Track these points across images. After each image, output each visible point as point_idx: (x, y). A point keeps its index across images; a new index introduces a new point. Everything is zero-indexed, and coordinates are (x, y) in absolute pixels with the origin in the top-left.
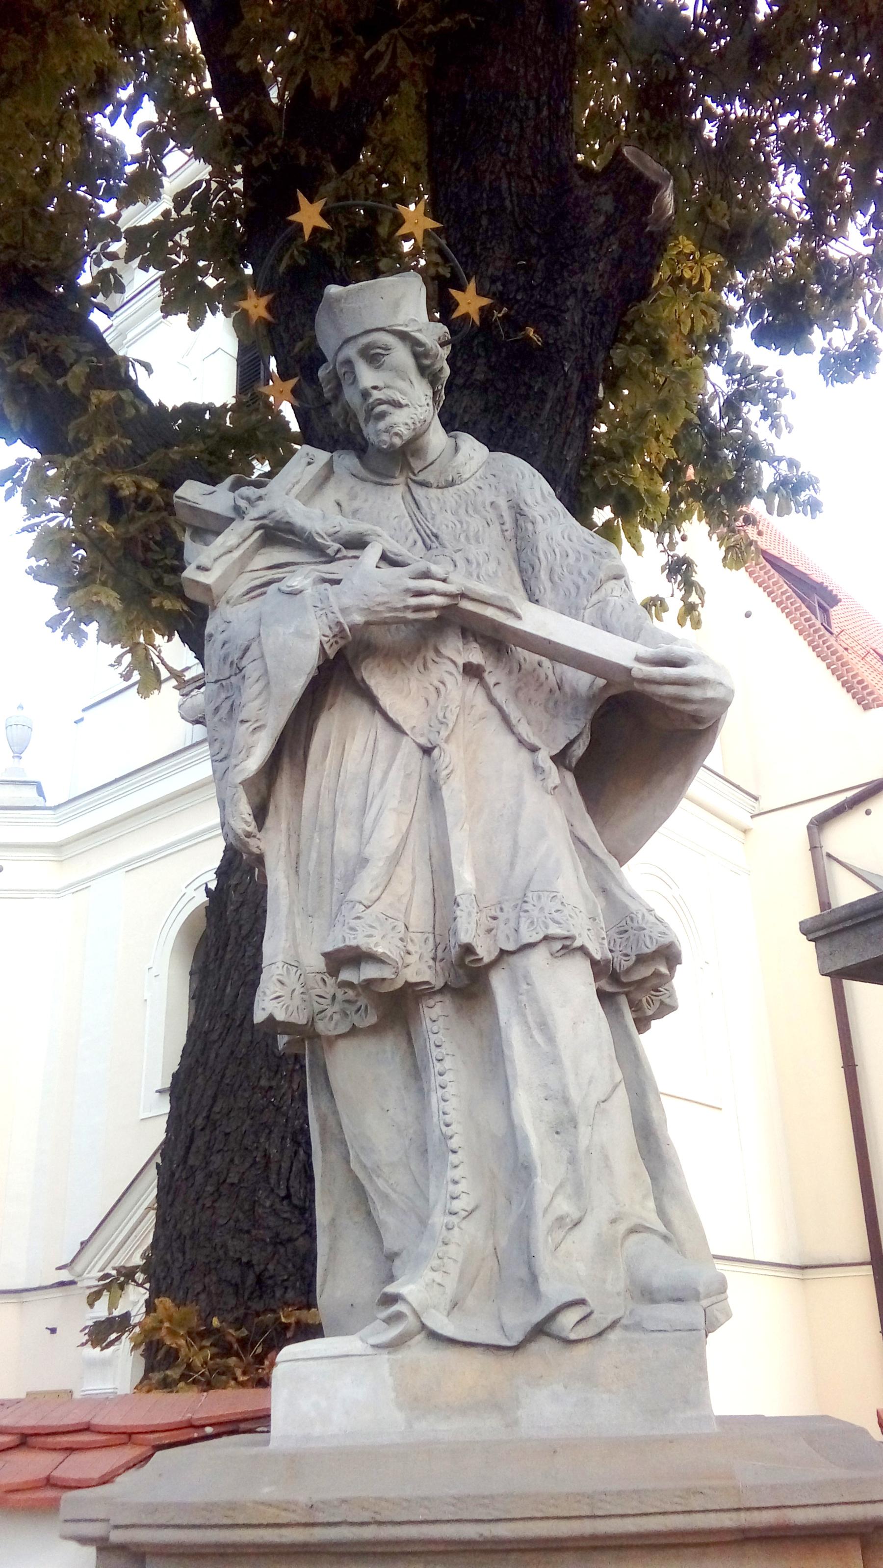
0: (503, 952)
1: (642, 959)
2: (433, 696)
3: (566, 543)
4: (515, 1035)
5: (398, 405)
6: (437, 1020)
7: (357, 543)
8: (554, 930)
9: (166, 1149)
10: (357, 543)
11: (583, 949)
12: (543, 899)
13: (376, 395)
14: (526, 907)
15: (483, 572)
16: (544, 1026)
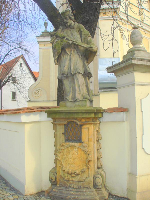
0: (74, 74)
1: (88, 73)
4: (75, 80)
5: (68, 23)
7: (64, 37)
10: (64, 37)
11: (81, 73)
16: (78, 79)
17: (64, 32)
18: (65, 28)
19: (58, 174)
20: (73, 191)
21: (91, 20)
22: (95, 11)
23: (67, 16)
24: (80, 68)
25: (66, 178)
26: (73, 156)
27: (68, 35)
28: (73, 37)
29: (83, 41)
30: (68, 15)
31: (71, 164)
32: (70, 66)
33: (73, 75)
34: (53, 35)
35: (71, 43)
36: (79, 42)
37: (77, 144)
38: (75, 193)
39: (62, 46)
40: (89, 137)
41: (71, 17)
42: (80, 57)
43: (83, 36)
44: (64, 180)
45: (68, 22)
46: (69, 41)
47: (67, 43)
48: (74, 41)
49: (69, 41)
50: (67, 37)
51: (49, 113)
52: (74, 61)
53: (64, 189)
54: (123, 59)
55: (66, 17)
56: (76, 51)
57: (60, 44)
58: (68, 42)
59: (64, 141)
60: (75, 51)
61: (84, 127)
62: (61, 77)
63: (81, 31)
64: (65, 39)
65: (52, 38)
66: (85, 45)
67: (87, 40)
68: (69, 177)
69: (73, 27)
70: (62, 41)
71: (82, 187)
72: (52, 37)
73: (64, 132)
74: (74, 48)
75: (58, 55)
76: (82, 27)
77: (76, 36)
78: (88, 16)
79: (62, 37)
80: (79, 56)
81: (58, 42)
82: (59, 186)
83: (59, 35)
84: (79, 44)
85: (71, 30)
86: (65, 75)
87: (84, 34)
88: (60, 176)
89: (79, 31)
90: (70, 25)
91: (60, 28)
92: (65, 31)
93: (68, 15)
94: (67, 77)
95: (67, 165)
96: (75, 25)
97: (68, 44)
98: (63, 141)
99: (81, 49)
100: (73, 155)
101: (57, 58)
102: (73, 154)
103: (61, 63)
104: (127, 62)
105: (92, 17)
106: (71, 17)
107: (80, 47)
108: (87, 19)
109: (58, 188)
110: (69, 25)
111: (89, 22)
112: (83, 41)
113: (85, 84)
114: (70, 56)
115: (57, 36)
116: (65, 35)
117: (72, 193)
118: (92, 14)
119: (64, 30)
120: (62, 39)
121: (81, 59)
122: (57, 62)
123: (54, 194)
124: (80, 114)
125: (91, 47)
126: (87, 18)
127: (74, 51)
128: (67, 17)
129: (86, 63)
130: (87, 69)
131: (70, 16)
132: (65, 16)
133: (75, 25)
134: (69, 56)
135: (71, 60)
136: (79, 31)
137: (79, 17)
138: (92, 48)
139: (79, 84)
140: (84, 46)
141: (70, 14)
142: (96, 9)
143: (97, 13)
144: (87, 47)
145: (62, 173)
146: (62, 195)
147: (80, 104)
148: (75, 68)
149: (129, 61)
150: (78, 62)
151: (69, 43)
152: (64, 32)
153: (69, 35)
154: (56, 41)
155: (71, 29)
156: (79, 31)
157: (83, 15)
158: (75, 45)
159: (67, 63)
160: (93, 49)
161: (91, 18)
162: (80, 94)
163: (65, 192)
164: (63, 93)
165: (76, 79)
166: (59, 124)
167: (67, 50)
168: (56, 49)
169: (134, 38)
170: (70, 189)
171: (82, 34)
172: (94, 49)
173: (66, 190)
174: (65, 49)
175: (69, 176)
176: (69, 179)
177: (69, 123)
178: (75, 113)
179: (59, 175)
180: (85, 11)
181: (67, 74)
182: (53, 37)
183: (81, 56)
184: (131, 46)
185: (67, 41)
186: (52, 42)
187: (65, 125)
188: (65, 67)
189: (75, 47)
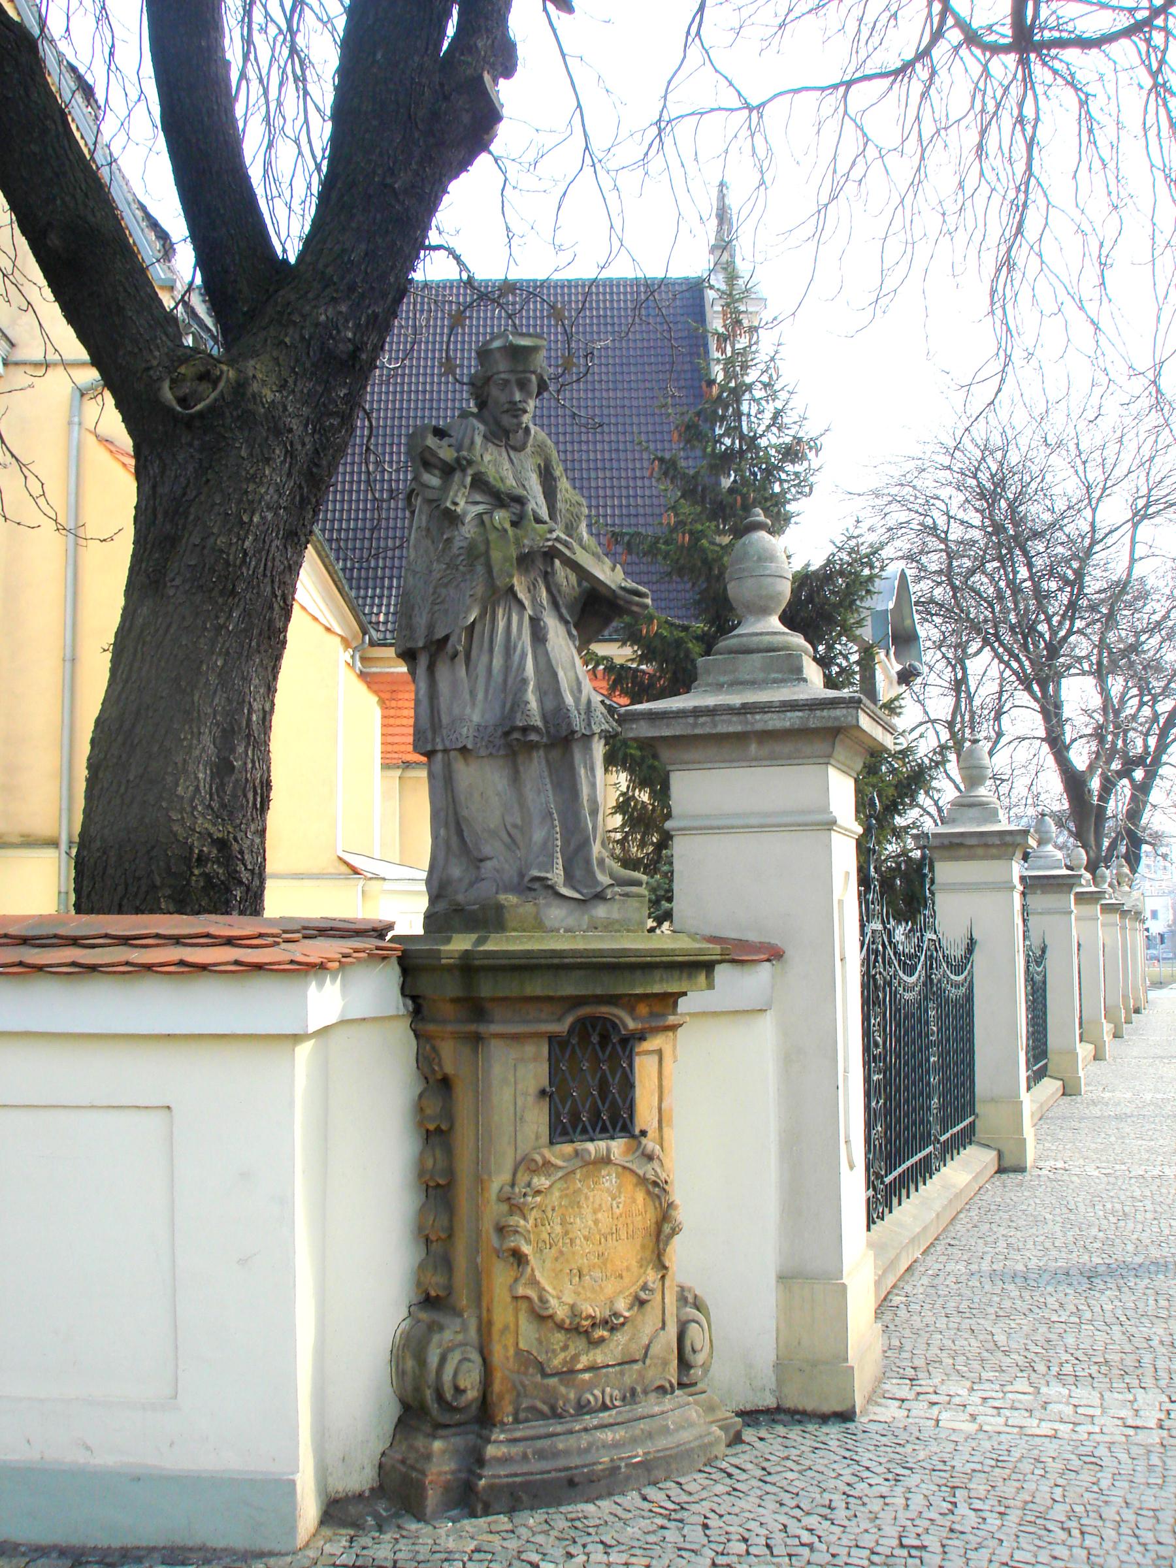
19: (505, 1347)
20: (606, 1426)
23: (534, 372)
25: (557, 1362)
26: (596, 1222)
31: (585, 1271)
37: (617, 1147)
38: (620, 1434)
40: (661, 1100)
44: (545, 1375)
53: (559, 1428)
55: (529, 380)
59: (545, 1139)
61: (647, 1045)
63: (551, 475)
68: (572, 1351)
71: (639, 1389)
73: (545, 1082)
82: (517, 1421)
88: (518, 1352)
95: (567, 1279)
98: (537, 1138)
100: (600, 1215)
102: (595, 1212)
104: (818, 713)
109: (518, 1434)
117: (608, 1436)
123: (516, 1475)
124: (657, 974)
126: (350, 335)
132: (524, 372)
144: (613, 586)
145: (528, 1335)
146: (562, 1463)
147: (616, 915)
149: (838, 712)
155: (515, 449)
163: (572, 1441)
164: (175, 816)
166: (515, 1038)
169: (770, 579)
170: (590, 1420)
173: (571, 1432)
175: (579, 1344)
176: (575, 1358)
177: (583, 1027)
178: (633, 967)
179: (511, 1352)
187: (552, 1039)
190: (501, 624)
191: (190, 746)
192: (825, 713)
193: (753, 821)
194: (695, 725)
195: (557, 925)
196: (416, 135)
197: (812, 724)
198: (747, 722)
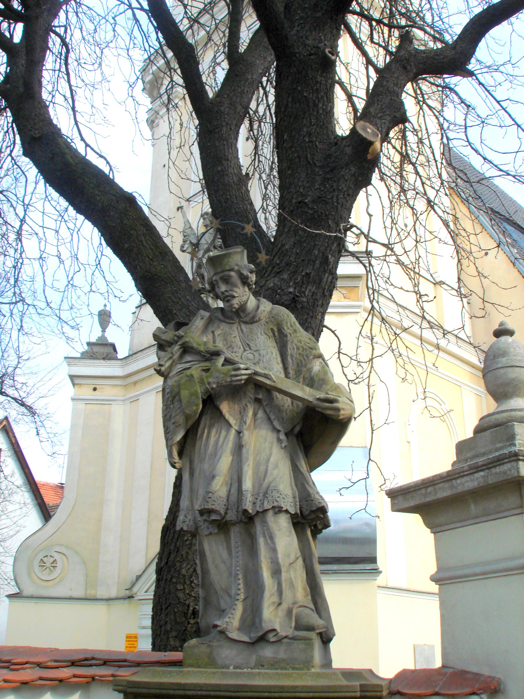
0: (258, 512)
1: (312, 512)
2: (242, 411)
3: (299, 344)
4: (261, 541)
5: (234, 297)
6: (235, 533)
7: (217, 354)
8: (276, 504)
9: (159, 553)
10: (217, 354)
11: (287, 511)
12: (274, 493)
13: (227, 294)
14: (267, 496)
15: (265, 360)
16: (272, 538)
17: (213, 332)
18: (220, 320)
21: (305, 300)
22: (322, 269)
23: (232, 270)
24: (281, 487)
27: (230, 347)
28: (251, 356)
29: (291, 372)
30: (236, 268)
32: (235, 477)
33: (249, 520)
34: (170, 344)
35: (247, 380)
36: (278, 377)
39: (207, 391)
41: (247, 278)
42: (279, 440)
43: (292, 356)
45: (235, 294)
46: (239, 369)
47: (229, 379)
48: (256, 373)
49: (239, 369)
50: (229, 354)
51: (131, 693)
52: (252, 454)
54: (457, 454)
55: (230, 276)
56: (265, 411)
57: (197, 380)
58: (233, 373)
60: (260, 414)
62: (192, 522)
63: (283, 333)
64: (221, 360)
65: (162, 354)
66: (303, 390)
67: (310, 370)
69: (253, 317)
70: (207, 370)
72: (166, 351)
74: (258, 401)
75: (188, 428)
76: (289, 318)
77: (262, 352)
78: (294, 283)
79: (207, 352)
80: (275, 435)
81: (188, 372)
83: (195, 345)
84: (279, 386)
85: (243, 326)
86: (214, 517)
87: (298, 348)
89: (276, 334)
90: (243, 308)
91: (199, 318)
92: (220, 330)
93: (236, 268)
94: (223, 526)
96: (259, 311)
97: (232, 381)
99: (286, 406)
101: (181, 439)
103: (196, 461)
104: (493, 470)
105: (310, 290)
106: (250, 275)
107: (280, 396)
108: (292, 296)
110: (237, 306)
111: (299, 306)
112: (291, 375)
113: (300, 562)
114: (239, 433)
115: (186, 349)
116: (220, 345)
118: (311, 280)
119: (216, 325)
120: (207, 360)
121: (285, 446)
122: (181, 454)
125: (331, 401)
126: (291, 290)
127: (255, 415)
128: (233, 274)
129: (303, 466)
130: (309, 492)
131: (245, 272)
132: (223, 271)
133: (262, 308)
134: (233, 432)
135: (244, 451)
136: (274, 334)
137: (262, 284)
138: (335, 405)
139: (277, 558)
140: (298, 393)
141: (245, 266)
142: (326, 261)
143: (327, 275)
144: (311, 399)
147: (282, 655)
148: (261, 485)
149: (505, 467)
150: (272, 460)
151: (239, 378)
152: (216, 333)
153: (233, 344)
154: (180, 367)
155: (245, 323)
156: (274, 334)
157: (276, 280)
158: (259, 386)
159: (225, 462)
160: (338, 410)
161: (304, 292)
162: (280, 604)
164: (180, 587)
165: (264, 536)
167: (225, 407)
168: (180, 401)
169: (502, 371)
171: (289, 346)
172: (343, 409)
174: (218, 404)
180: (283, 264)
181: (222, 512)
182: (169, 349)
183: (287, 434)
184: (489, 405)
185: (230, 370)
186: (163, 369)
188: (215, 481)
189: (260, 396)
190: (213, 439)
191: (191, 544)
192: (498, 470)
193: (478, 570)
194: (425, 495)
195: (227, 662)
196: (317, 170)
197: (492, 480)
198: (452, 487)
